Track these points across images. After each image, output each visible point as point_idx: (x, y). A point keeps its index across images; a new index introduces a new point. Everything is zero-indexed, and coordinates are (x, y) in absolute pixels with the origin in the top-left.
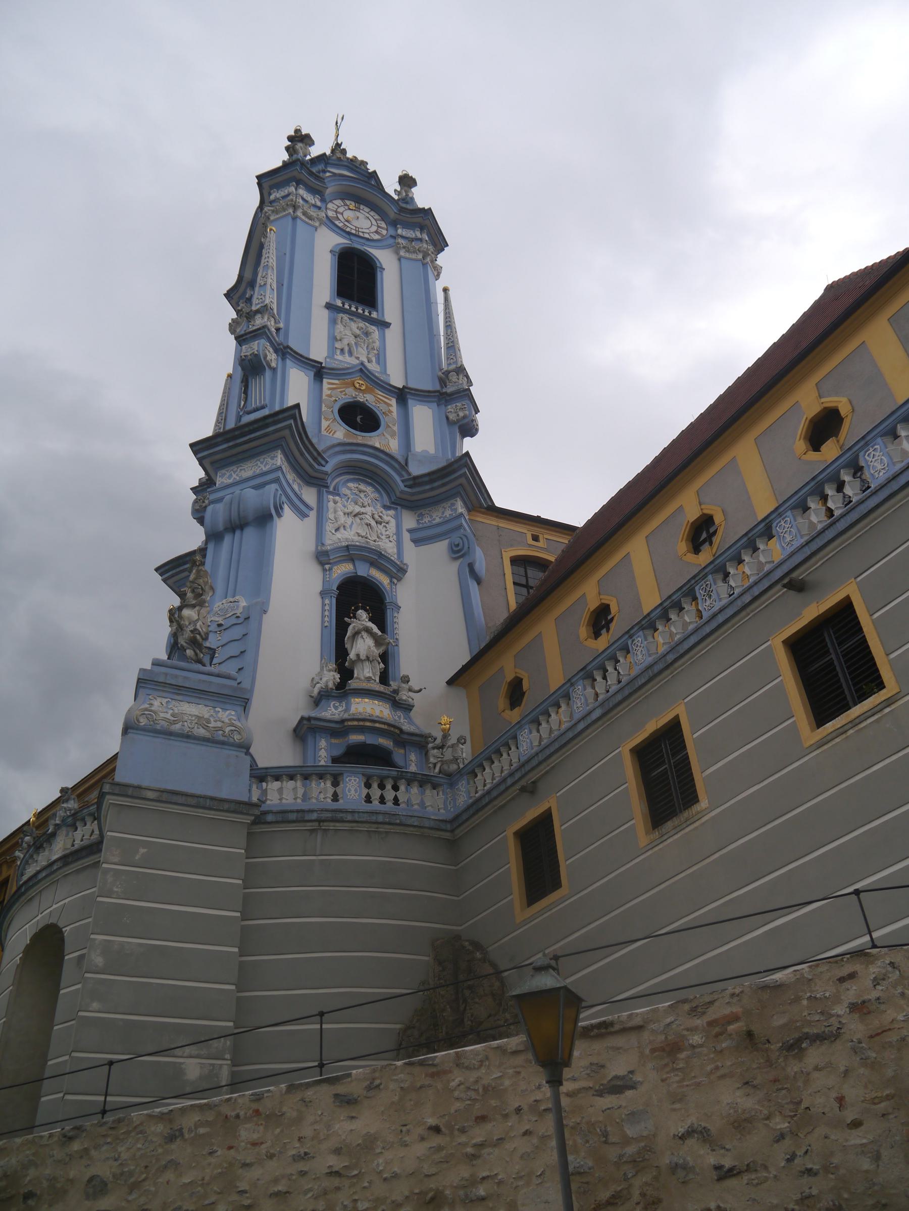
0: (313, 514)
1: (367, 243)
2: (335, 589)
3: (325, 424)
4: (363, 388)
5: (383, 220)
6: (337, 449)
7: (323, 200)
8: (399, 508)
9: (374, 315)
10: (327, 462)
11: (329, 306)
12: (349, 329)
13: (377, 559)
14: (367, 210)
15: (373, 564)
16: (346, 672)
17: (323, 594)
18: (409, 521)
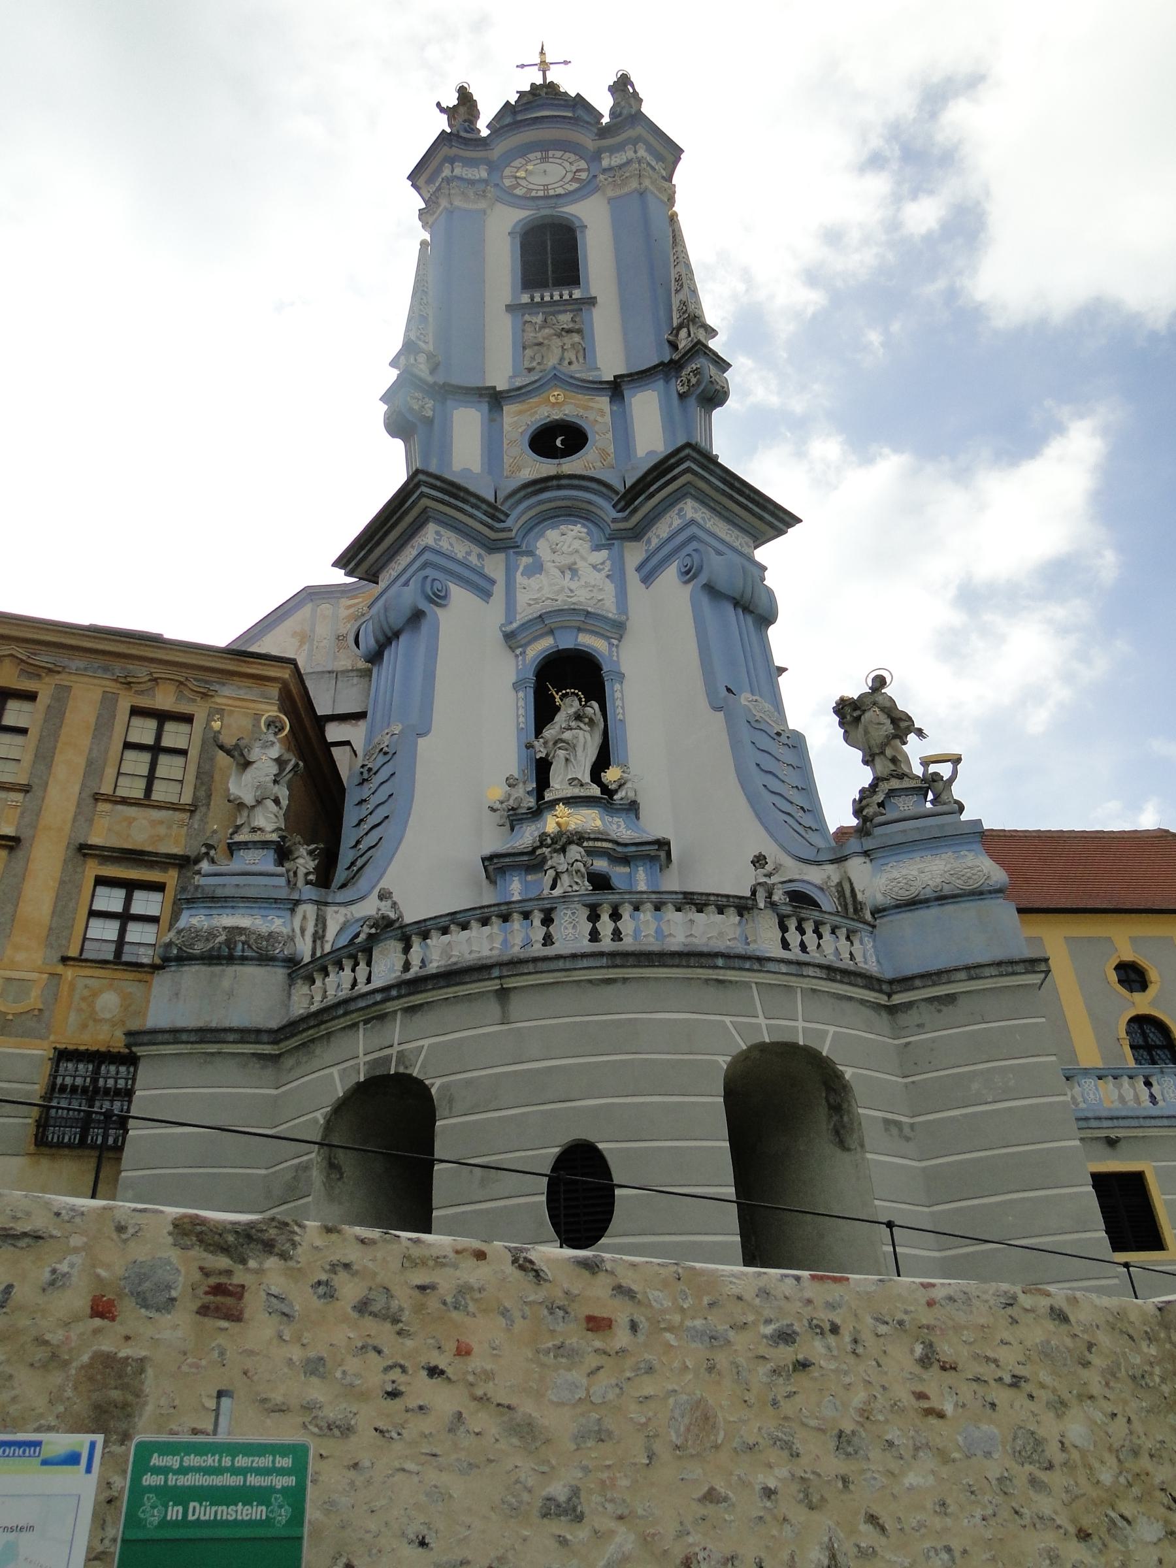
1: (561, 201)
2: (531, 677)
4: (561, 398)
5: (583, 159)
6: (518, 496)
7: (493, 167)
8: (615, 542)
9: (577, 294)
10: (507, 515)
11: (509, 308)
13: (586, 618)
14: (559, 154)
15: (579, 629)
17: (516, 686)
18: (634, 554)
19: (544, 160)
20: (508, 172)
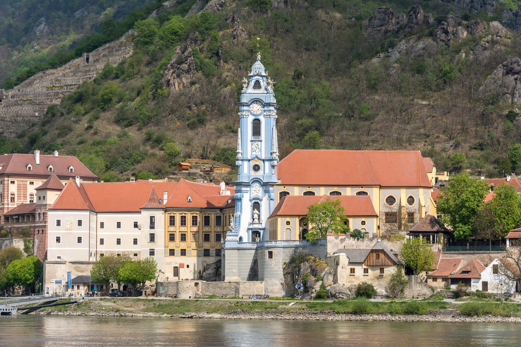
12: (255, 144)
13: (258, 199)
15: (257, 199)
16: (254, 219)
17: (251, 206)
19: (257, 103)
20: (251, 106)
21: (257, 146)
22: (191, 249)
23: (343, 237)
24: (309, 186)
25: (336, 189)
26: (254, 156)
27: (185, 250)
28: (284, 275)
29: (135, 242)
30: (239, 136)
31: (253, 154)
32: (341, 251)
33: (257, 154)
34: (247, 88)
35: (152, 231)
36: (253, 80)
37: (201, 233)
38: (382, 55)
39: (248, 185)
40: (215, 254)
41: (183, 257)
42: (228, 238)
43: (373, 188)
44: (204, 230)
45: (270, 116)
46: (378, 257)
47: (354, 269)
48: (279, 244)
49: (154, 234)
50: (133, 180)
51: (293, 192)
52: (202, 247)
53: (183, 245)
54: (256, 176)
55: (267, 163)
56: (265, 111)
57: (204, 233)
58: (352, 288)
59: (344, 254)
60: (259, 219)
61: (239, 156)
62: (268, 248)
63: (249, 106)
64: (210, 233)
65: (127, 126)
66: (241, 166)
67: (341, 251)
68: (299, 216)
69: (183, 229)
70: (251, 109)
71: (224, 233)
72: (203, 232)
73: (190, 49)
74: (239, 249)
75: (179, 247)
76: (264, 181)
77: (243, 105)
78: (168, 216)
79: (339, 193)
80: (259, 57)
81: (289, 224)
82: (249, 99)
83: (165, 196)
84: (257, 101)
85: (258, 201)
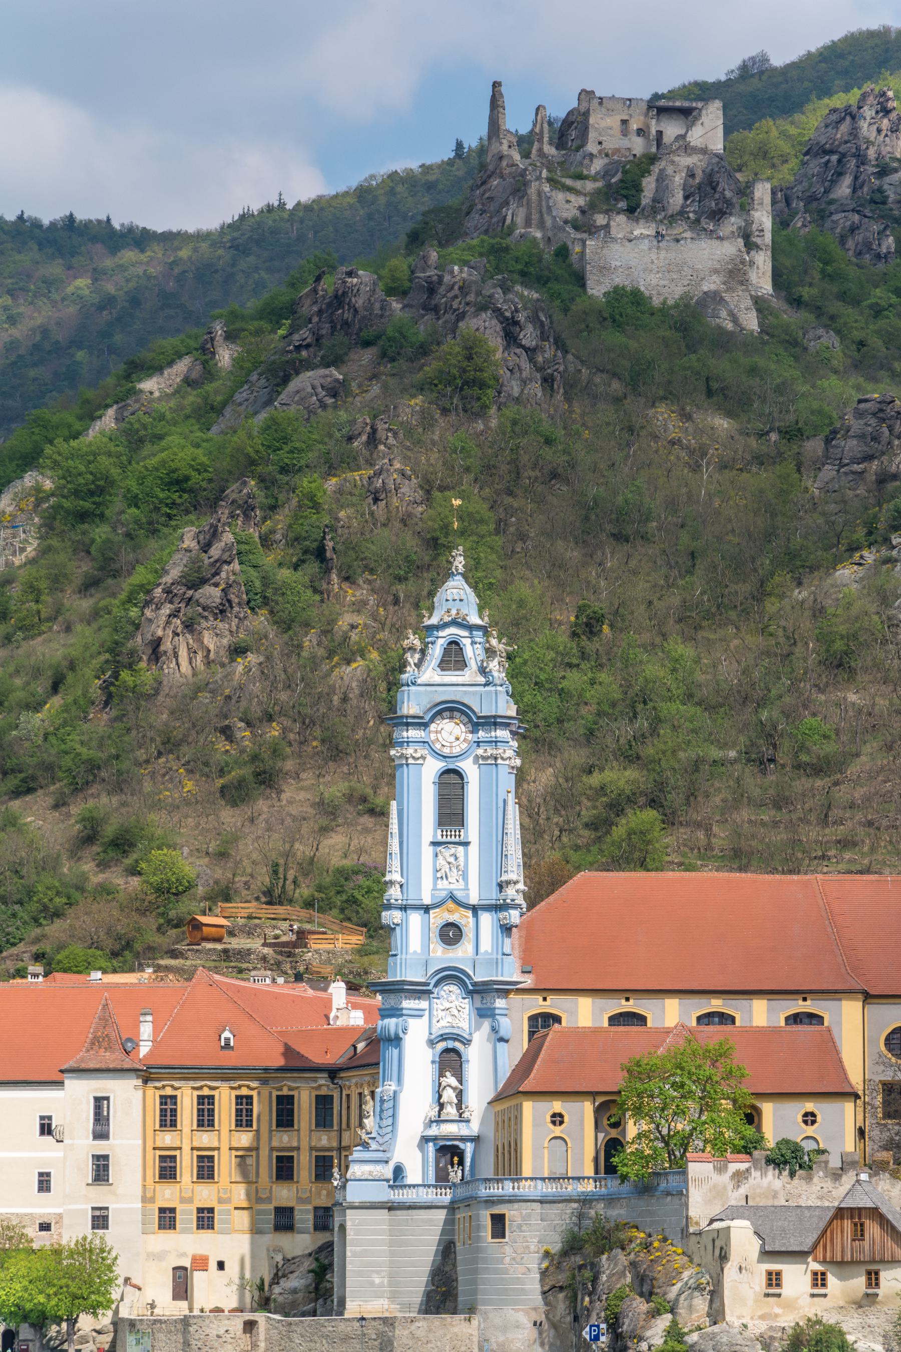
0: (427, 1013)
3: (432, 946)
12: (447, 852)
13: (456, 1038)
15: (455, 1039)
16: (441, 1106)
17: (433, 1062)
19: (451, 718)
20: (433, 727)
21: (452, 860)
22: (230, 1207)
23: (743, 1166)
24: (627, 993)
25: (716, 1004)
26: (444, 894)
27: (211, 1210)
28: (544, 1293)
29: (44, 1183)
30: (394, 827)
31: (439, 887)
32: (734, 1213)
33: (452, 887)
34: (418, 665)
35: (101, 1147)
36: (441, 642)
37: (264, 1152)
38: (869, 556)
39: (421, 991)
40: (310, 1225)
41: (205, 1235)
42: (356, 1170)
43: (840, 1000)
44: (275, 1144)
45: (496, 759)
46: (859, 1233)
47: (779, 1273)
48: (526, 1189)
49: (106, 1157)
50: (36, 975)
51: (574, 1013)
52: (269, 1200)
53: (205, 1195)
54: (451, 960)
55: (487, 920)
56: (478, 743)
57: (275, 1154)
58: (771, 1338)
59: (747, 1223)
60: (459, 1106)
61: (394, 893)
62: (490, 1202)
63: (425, 725)
64: (294, 1154)
65: (17, 793)
66: (398, 929)
67: (734, 1213)
68: (593, 1094)
69: (206, 1139)
70: (433, 736)
71: (344, 1153)
72: (272, 1149)
73: (228, 537)
74: (391, 1207)
75: (190, 1200)
76: (476, 979)
77: (407, 723)
78: (153, 1095)
79: (725, 1019)
80: (459, 563)
81: (561, 1123)
82: (426, 703)
83: (146, 1030)
84: (451, 710)
85: (458, 1045)
